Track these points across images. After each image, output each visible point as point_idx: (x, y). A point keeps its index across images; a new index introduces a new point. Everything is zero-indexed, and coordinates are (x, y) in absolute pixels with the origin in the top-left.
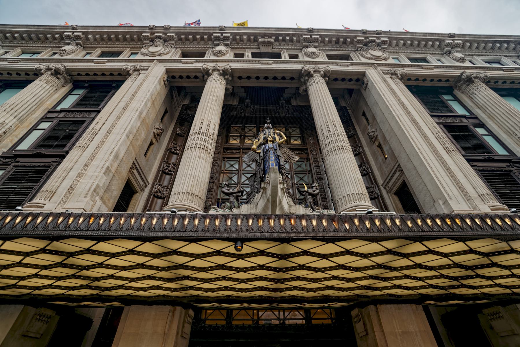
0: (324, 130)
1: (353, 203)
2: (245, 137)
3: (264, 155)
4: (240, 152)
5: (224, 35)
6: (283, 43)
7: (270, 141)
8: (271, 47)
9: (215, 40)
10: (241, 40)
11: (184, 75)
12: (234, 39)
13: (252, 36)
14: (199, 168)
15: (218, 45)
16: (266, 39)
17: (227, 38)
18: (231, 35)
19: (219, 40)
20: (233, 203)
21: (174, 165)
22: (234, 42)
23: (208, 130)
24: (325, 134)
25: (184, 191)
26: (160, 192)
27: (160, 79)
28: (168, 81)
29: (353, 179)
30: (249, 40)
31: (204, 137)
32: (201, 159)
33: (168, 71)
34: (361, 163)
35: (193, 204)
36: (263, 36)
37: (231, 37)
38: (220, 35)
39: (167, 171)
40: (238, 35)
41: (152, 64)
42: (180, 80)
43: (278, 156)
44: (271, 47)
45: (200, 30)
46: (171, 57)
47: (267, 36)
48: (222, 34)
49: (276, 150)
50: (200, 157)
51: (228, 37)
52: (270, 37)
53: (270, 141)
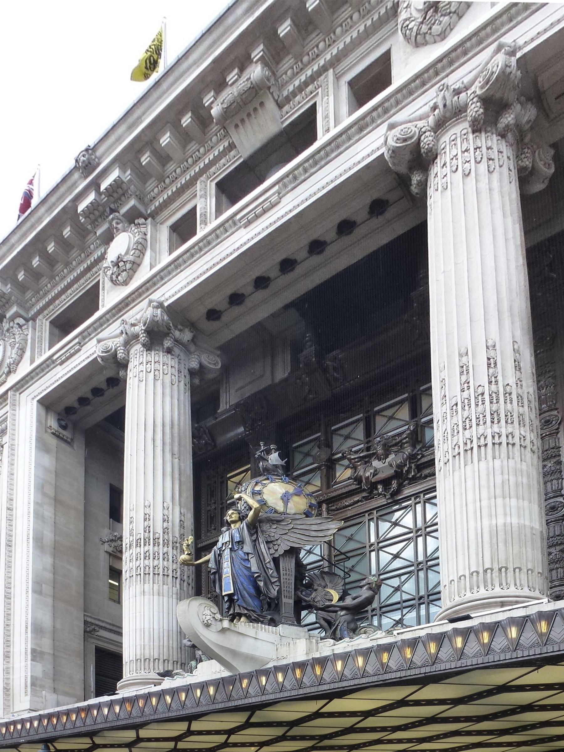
5: (103, 187)
6: (315, 40)
8: (270, 105)
9: (95, 223)
10: (163, 158)
11: (85, 391)
12: (143, 174)
13: (182, 113)
15: (108, 238)
16: (237, 85)
17: (118, 191)
18: (123, 170)
19: (103, 216)
22: (151, 184)
27: (39, 439)
28: (61, 426)
30: (184, 137)
33: (47, 404)
36: (215, 79)
37: (127, 176)
38: (91, 197)
40: (140, 152)
41: (7, 408)
42: (89, 408)
44: (270, 105)
45: (40, 220)
46: (32, 361)
47: (229, 69)
48: (95, 184)
51: (118, 184)
52: (243, 63)
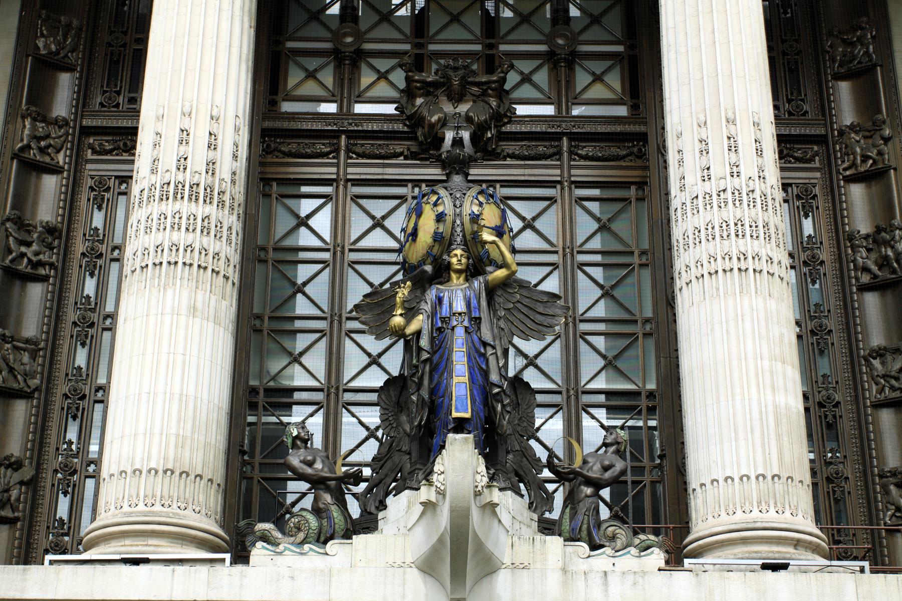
0: (687, 157)
1: (739, 512)
2: (359, 57)
3: (432, 339)
4: (337, 151)
7: (459, 272)
14: (194, 360)
20: (329, 518)
21: (51, 230)
23: (211, 166)
24: (689, 180)
25: (153, 465)
26: (11, 370)
29: (756, 415)
31: (201, 210)
32: (198, 320)
34: (879, 230)
35: (188, 512)
39: (23, 266)
43: (485, 344)
49: (478, 320)
50: (193, 310)
53: (459, 272)
